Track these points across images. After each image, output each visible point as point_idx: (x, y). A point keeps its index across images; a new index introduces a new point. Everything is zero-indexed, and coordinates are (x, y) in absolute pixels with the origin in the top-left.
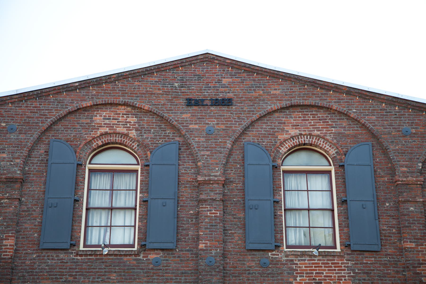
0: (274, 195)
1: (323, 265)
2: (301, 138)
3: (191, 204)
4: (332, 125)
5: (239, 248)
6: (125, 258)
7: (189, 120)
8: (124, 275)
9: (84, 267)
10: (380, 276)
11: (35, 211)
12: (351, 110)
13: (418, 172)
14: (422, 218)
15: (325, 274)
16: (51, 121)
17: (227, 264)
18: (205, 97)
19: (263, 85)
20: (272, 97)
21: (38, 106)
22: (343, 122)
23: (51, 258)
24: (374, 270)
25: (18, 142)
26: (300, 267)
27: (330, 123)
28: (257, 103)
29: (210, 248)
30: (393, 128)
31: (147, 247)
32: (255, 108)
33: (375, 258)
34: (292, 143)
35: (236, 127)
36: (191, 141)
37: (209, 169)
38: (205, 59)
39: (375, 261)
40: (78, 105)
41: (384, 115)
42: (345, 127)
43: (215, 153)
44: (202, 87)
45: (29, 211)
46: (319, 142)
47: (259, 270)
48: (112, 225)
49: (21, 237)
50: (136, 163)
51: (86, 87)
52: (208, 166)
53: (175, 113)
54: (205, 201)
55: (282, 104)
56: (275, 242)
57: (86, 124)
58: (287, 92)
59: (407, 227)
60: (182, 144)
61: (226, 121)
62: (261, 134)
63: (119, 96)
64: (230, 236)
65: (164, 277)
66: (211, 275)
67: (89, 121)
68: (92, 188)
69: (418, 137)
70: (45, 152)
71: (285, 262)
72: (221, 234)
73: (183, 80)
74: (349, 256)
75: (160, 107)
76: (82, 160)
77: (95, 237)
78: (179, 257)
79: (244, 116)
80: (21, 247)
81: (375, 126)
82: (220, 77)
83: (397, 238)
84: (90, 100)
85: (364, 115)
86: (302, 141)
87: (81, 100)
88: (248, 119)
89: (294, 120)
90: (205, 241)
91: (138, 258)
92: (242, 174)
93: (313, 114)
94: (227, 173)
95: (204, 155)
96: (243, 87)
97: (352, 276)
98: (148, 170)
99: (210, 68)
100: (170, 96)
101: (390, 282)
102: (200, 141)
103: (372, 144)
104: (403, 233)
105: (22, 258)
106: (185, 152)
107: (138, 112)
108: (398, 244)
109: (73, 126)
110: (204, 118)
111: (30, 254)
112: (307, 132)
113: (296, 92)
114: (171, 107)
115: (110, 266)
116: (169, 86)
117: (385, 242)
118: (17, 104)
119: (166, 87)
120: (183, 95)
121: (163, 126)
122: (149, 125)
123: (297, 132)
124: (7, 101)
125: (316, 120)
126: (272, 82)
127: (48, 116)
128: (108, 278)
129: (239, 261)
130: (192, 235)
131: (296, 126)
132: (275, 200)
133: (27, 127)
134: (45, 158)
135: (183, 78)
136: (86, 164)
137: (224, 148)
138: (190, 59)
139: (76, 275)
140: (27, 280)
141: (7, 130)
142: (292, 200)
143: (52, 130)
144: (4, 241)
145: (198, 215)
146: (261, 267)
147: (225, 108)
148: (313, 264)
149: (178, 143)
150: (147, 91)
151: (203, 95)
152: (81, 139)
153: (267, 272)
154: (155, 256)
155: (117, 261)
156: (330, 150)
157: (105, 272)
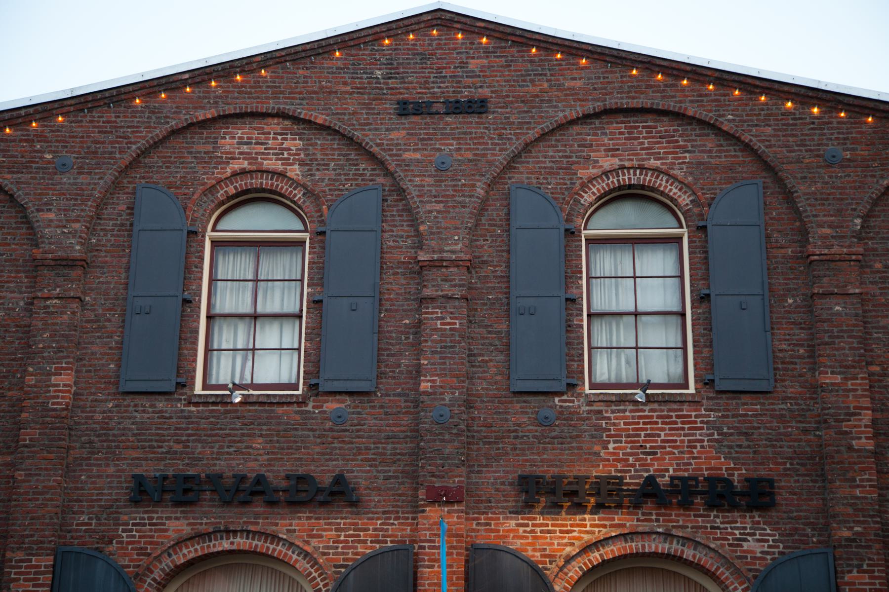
0: (567, 287)
1: (660, 421)
2: (624, 175)
3: (406, 307)
4: (686, 146)
5: (497, 389)
6: (280, 410)
7: (402, 142)
8: (278, 442)
9: (202, 426)
10: (770, 440)
11: (109, 321)
12: (724, 116)
13: (854, 237)
14: (857, 326)
15: (663, 438)
16: (138, 148)
17: (473, 419)
18: (433, 98)
19: (549, 70)
20: (566, 95)
21: (113, 119)
22: (707, 140)
23: (141, 409)
24: (759, 428)
25: (76, 189)
26: (614, 424)
27: (681, 143)
28: (537, 107)
29: (442, 390)
30: (806, 151)
31: (321, 389)
32: (533, 117)
33: (763, 404)
34: (604, 185)
35: (495, 155)
36: (407, 185)
37: (441, 239)
38: (435, 22)
39: (761, 410)
40: (188, 117)
41: (788, 125)
42: (710, 151)
43: (454, 207)
44: (429, 77)
45: (99, 321)
46: (659, 182)
47: (536, 431)
48: (257, 347)
49: (84, 369)
50: (302, 228)
51: (203, 81)
52: (439, 233)
53: (376, 129)
54: (433, 299)
55: (585, 108)
56: (567, 377)
57: (205, 153)
58: (597, 83)
59: (827, 344)
60: (389, 191)
61: (475, 144)
62: (545, 168)
63: (266, 98)
64: (480, 366)
65: (354, 446)
66: (443, 441)
67: (210, 148)
68: (219, 278)
69: (855, 167)
70: (128, 208)
71: (585, 415)
72: (463, 364)
73: (391, 64)
74: (711, 402)
75: (346, 117)
76: (197, 223)
77: (225, 370)
78: (382, 407)
79: (511, 134)
80: (86, 389)
81: (770, 146)
82: (464, 56)
83: (807, 367)
84: (210, 108)
85: (748, 125)
86: (624, 180)
87: (195, 108)
88: (518, 139)
89: (610, 139)
90: (432, 376)
91: (304, 408)
92: (505, 248)
93: (648, 127)
94: (476, 246)
95: (432, 212)
96: (508, 75)
97: (716, 440)
98: (323, 242)
99: (446, 39)
100: (366, 97)
101: (790, 450)
102: (423, 183)
103: (764, 182)
104: (820, 355)
105: (88, 409)
106: (394, 206)
107: (304, 129)
108: (809, 376)
109: (181, 157)
110: (431, 139)
111: (101, 401)
112: (636, 163)
113: (614, 82)
114: (368, 119)
115: (252, 423)
116: (365, 76)
117: (784, 375)
118: (75, 116)
119: (358, 78)
120: (392, 94)
121: (352, 157)
122: (327, 155)
123: (616, 162)
124: (54, 112)
125: (653, 137)
126: (567, 64)
127: (132, 140)
128: (247, 447)
129: (496, 413)
130: (407, 366)
131: (612, 151)
132: (568, 296)
133: (93, 162)
134: (127, 220)
135: (391, 59)
136: (205, 231)
137: (471, 196)
138: (406, 22)
139: (188, 441)
140: (96, 451)
141: (55, 168)
142: (604, 297)
143: (139, 167)
144: (53, 378)
145: (419, 327)
146: (541, 425)
147: (474, 119)
148: (640, 417)
149: (380, 189)
150: (321, 88)
151: (430, 93)
152: (195, 182)
153: (550, 435)
154: (336, 405)
155: (265, 415)
156: (680, 196)
157: (243, 435)
